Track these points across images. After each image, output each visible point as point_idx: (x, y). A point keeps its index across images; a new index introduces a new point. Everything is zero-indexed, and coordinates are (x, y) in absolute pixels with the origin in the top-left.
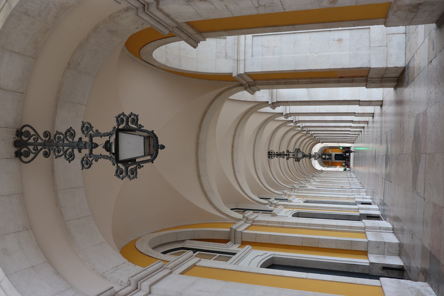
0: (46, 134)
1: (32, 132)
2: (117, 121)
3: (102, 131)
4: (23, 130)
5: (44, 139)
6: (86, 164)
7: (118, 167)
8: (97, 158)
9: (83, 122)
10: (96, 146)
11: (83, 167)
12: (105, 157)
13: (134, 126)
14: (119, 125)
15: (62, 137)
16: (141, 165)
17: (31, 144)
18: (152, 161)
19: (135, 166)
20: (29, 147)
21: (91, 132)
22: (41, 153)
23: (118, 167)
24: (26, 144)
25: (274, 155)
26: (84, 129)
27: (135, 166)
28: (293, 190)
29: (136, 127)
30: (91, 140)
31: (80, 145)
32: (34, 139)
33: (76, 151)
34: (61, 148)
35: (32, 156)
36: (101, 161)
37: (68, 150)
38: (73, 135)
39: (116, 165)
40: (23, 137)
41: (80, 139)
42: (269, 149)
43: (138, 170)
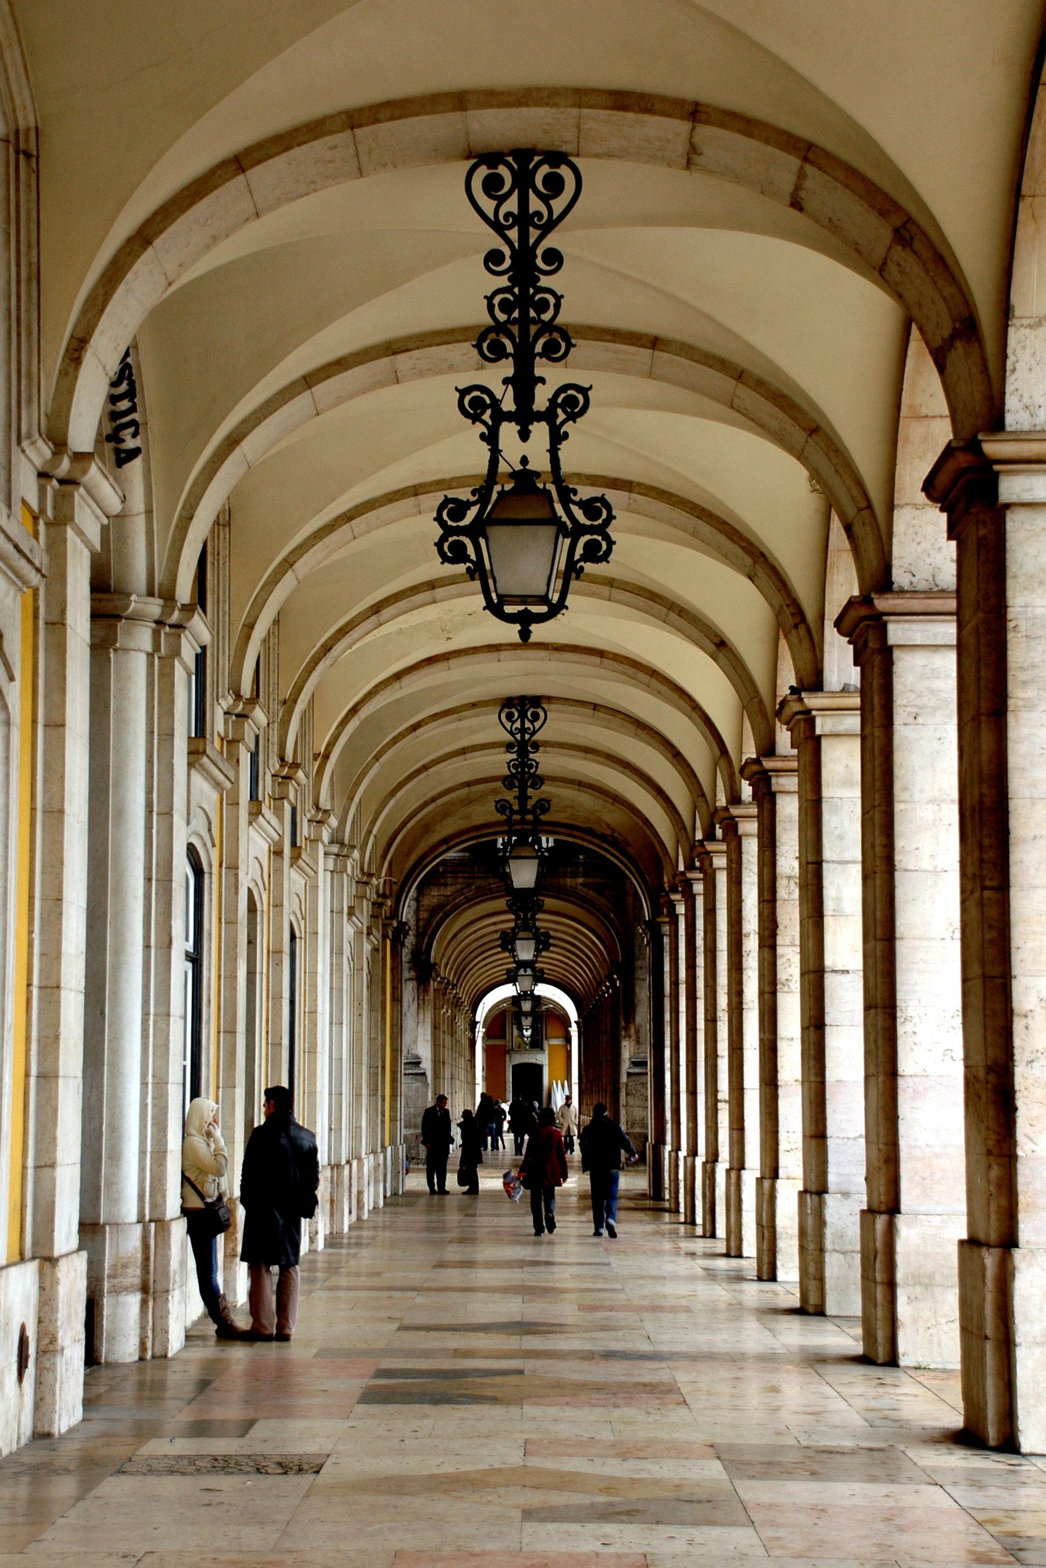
0: (554, 257)
1: (558, 205)
2: (595, 499)
3: (565, 450)
4: (565, 171)
5: (539, 252)
6: (475, 405)
7: (468, 505)
8: (491, 438)
9: (591, 387)
10: (524, 435)
11: (463, 393)
12: (494, 462)
13: (579, 551)
14: (581, 504)
15: (546, 317)
16: (477, 575)
17: (523, 202)
18: (490, 606)
19: (473, 557)
20: (515, 195)
21: (562, 416)
22: (497, 242)
23: (468, 505)
24: (523, 182)
25: (523, 730)
26: (571, 392)
27: (473, 557)
28: (335, 849)
29: (577, 557)
30: (539, 417)
31: (524, 383)
32: (539, 214)
33: (507, 368)
34: (516, 314)
35: (488, 205)
36: (484, 450)
37: (511, 337)
38: (551, 352)
39: (473, 499)
40: (545, 169)
41: (543, 381)
42: (549, 699)
43: (461, 568)
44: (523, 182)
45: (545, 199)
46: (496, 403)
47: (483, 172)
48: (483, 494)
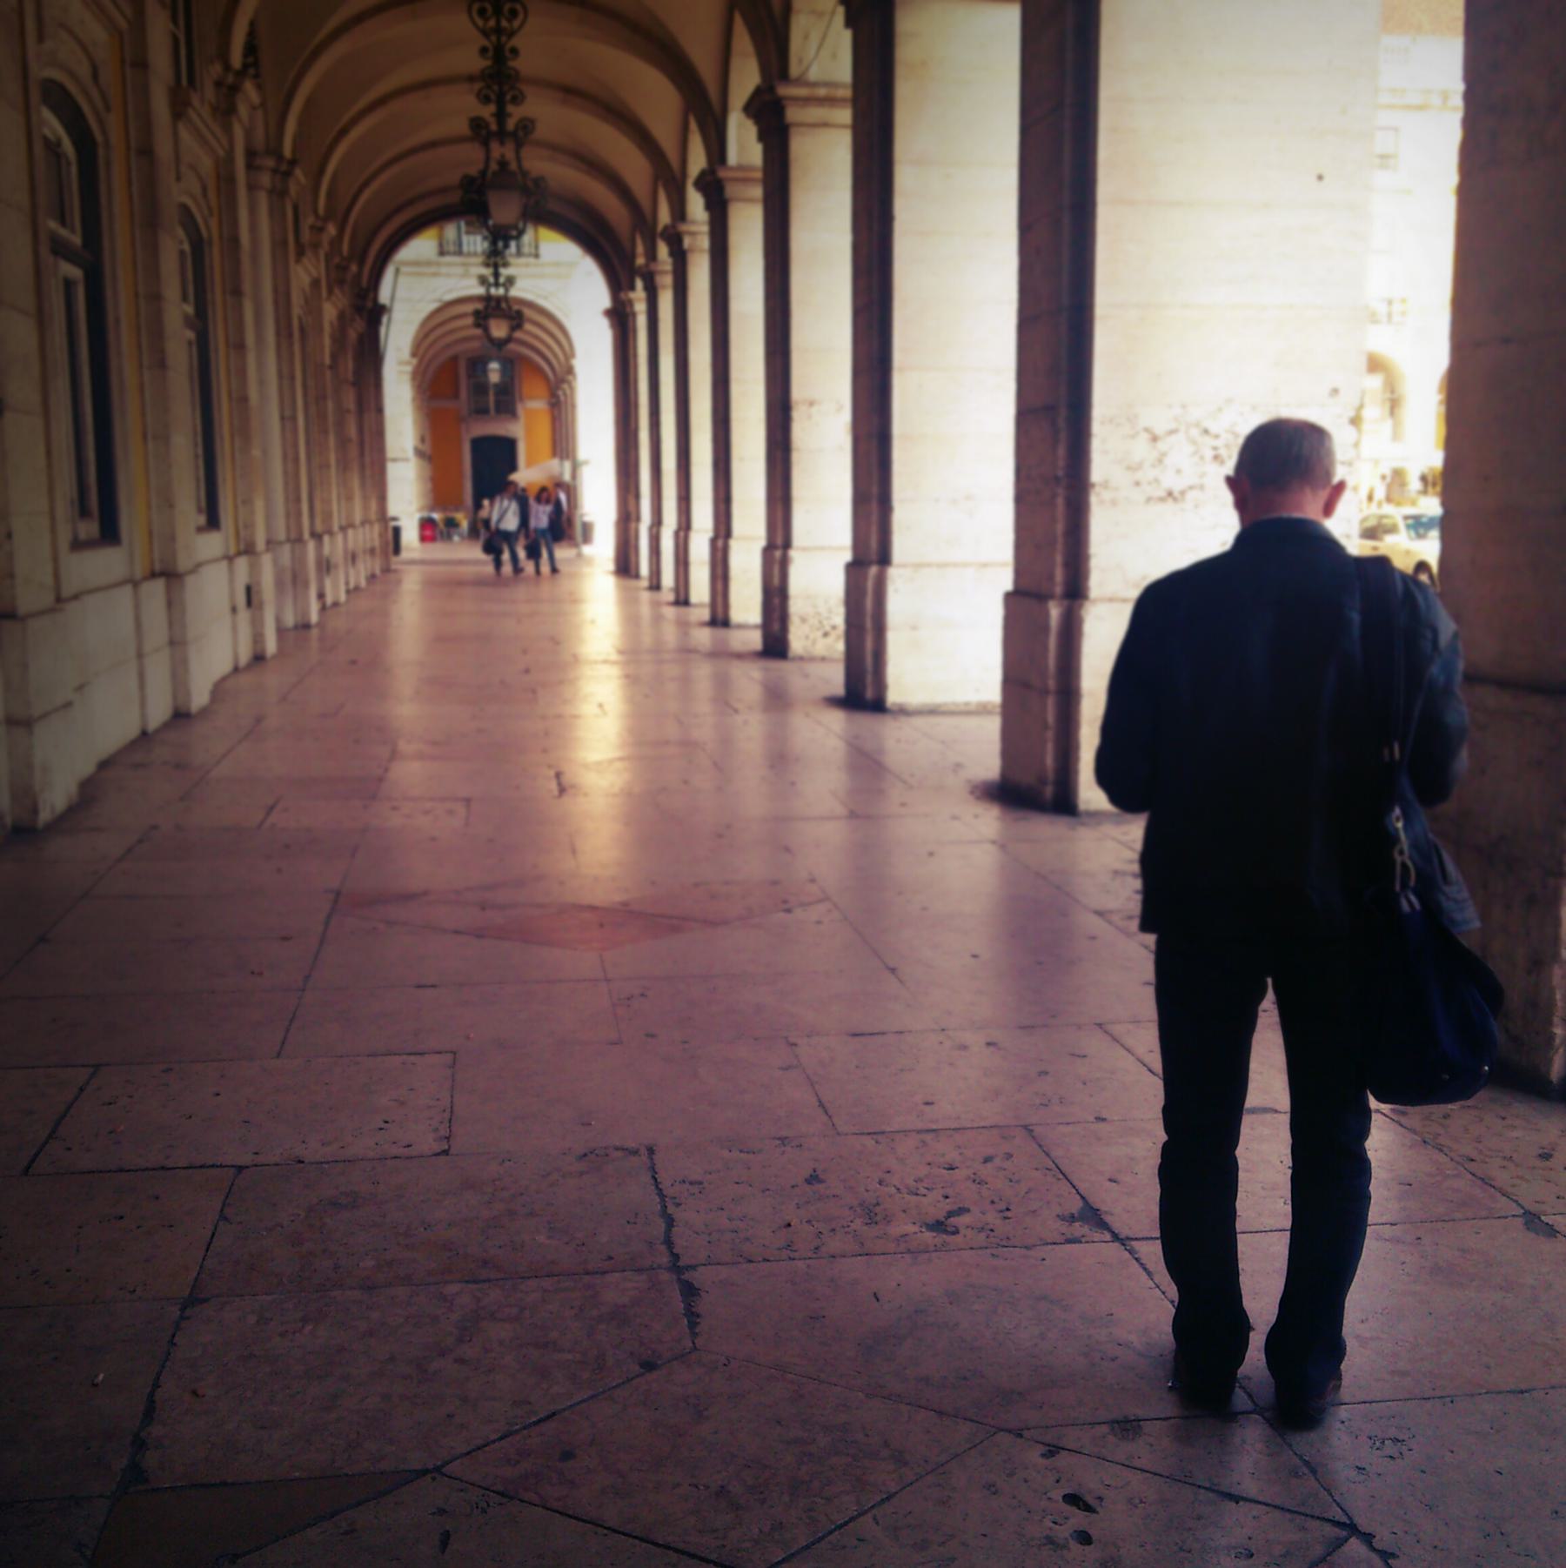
0: (515, 51)
1: (516, 23)
4: (518, 7)
6: (477, 124)
17: (498, 22)
31: (501, 115)
33: (492, 108)
35: (480, 22)
44: (498, 12)
45: (510, 21)
46: (487, 125)
47: (476, 6)
48: (483, 173)
